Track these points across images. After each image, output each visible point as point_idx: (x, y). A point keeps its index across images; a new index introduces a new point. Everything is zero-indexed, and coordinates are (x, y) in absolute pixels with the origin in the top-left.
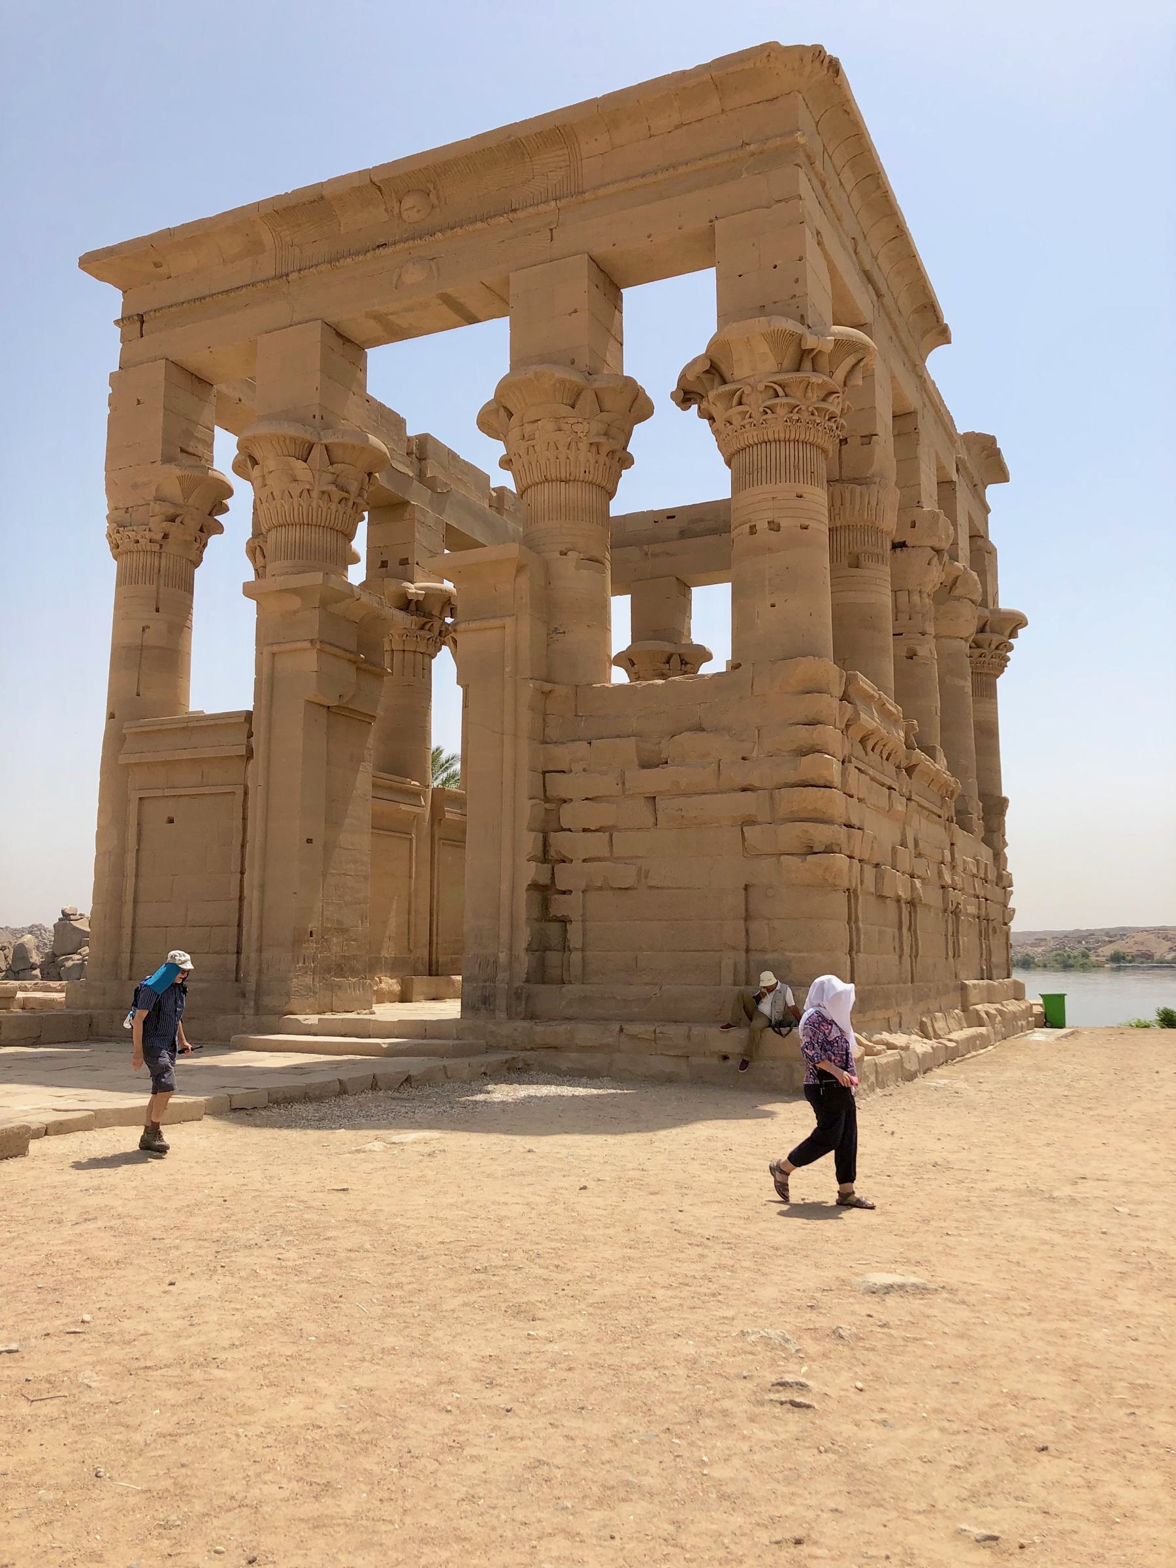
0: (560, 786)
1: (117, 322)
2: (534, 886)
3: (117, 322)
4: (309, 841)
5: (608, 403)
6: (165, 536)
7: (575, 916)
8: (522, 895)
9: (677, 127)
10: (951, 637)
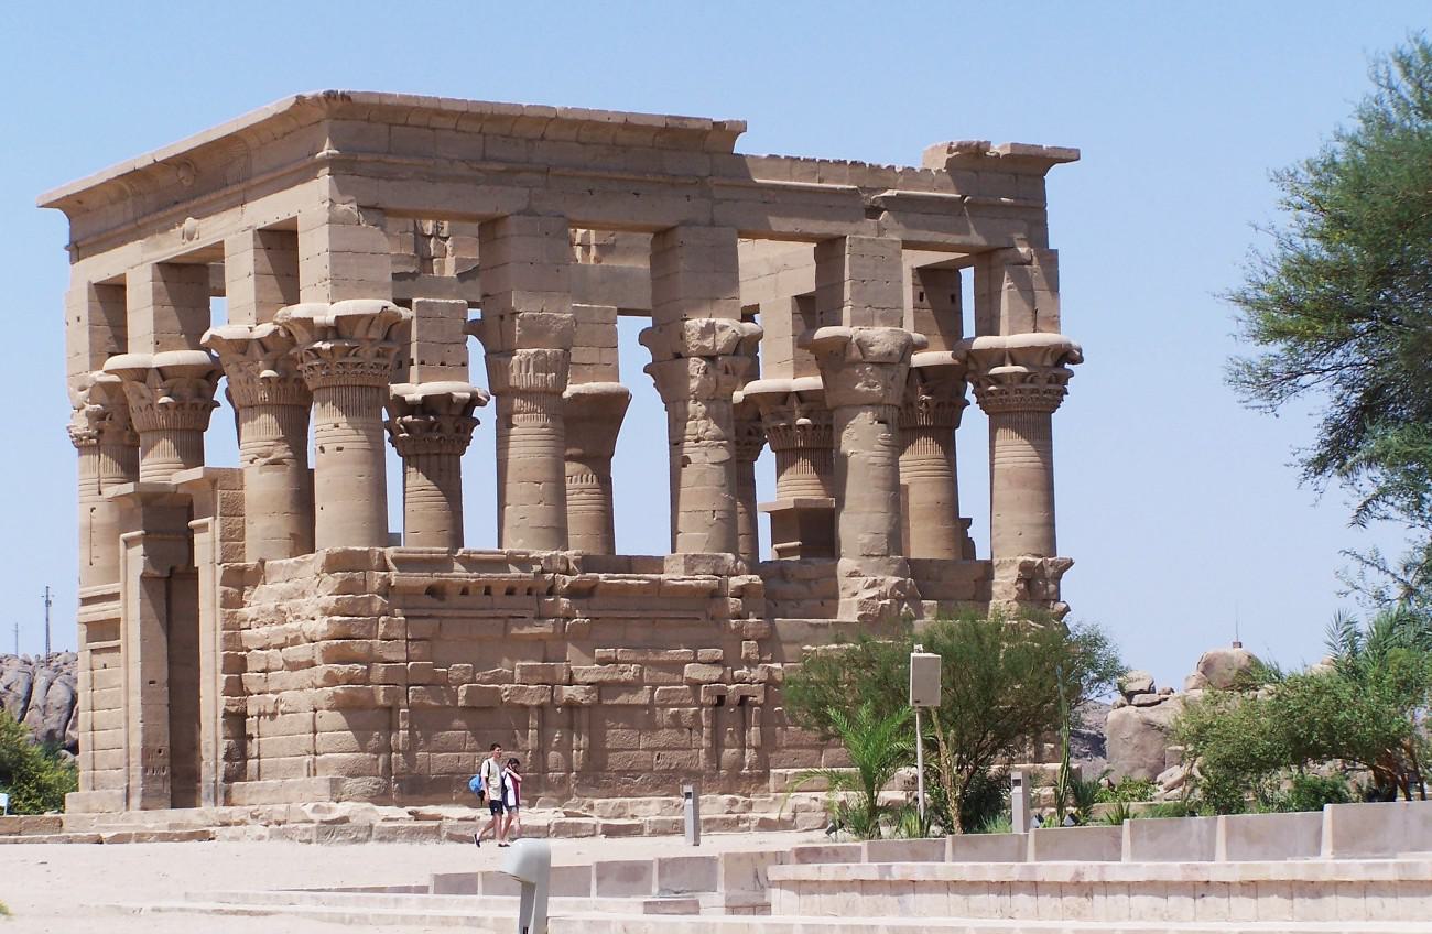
0: (252, 635)
1: (67, 248)
2: (226, 714)
3: (67, 248)
4: (151, 682)
5: (270, 345)
6: (100, 432)
7: (255, 735)
8: (220, 720)
9: (285, 134)
10: (849, 406)
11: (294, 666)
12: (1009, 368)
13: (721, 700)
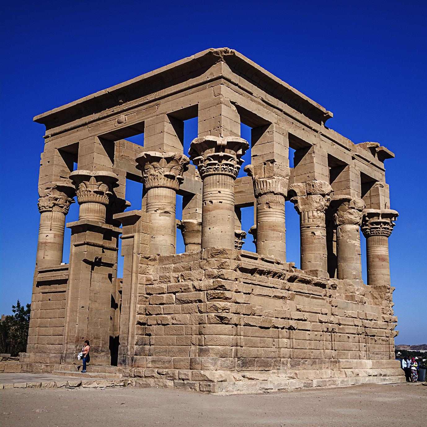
11: (181, 302)
12: (381, 220)
13: (328, 329)
